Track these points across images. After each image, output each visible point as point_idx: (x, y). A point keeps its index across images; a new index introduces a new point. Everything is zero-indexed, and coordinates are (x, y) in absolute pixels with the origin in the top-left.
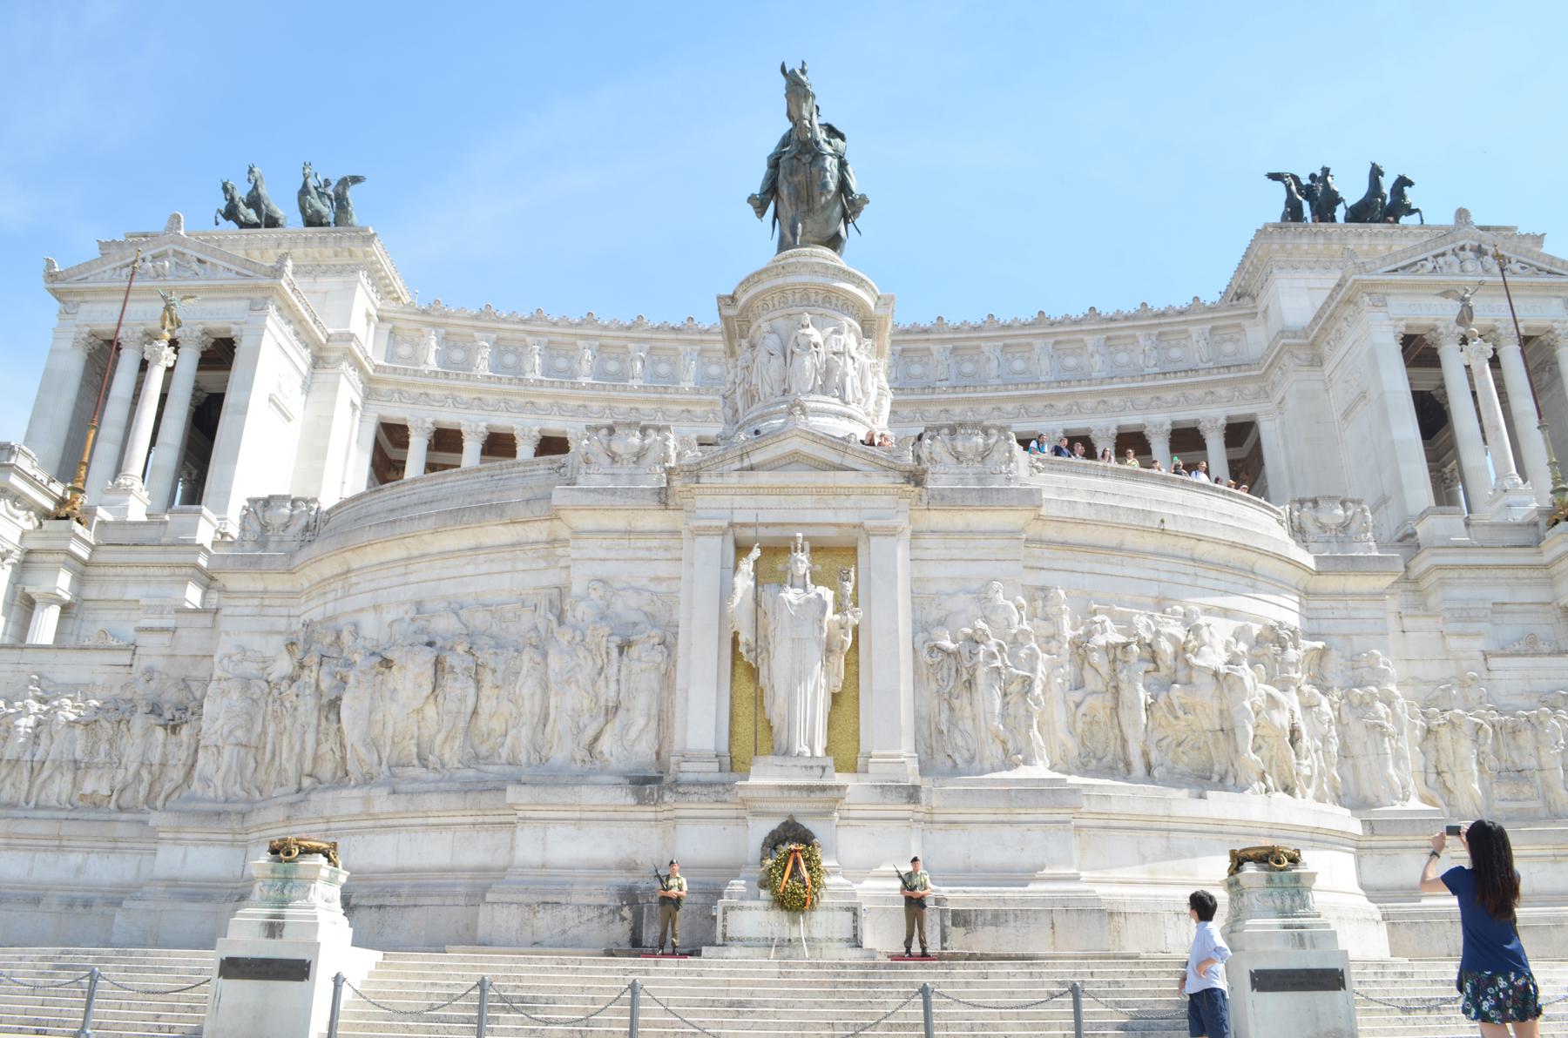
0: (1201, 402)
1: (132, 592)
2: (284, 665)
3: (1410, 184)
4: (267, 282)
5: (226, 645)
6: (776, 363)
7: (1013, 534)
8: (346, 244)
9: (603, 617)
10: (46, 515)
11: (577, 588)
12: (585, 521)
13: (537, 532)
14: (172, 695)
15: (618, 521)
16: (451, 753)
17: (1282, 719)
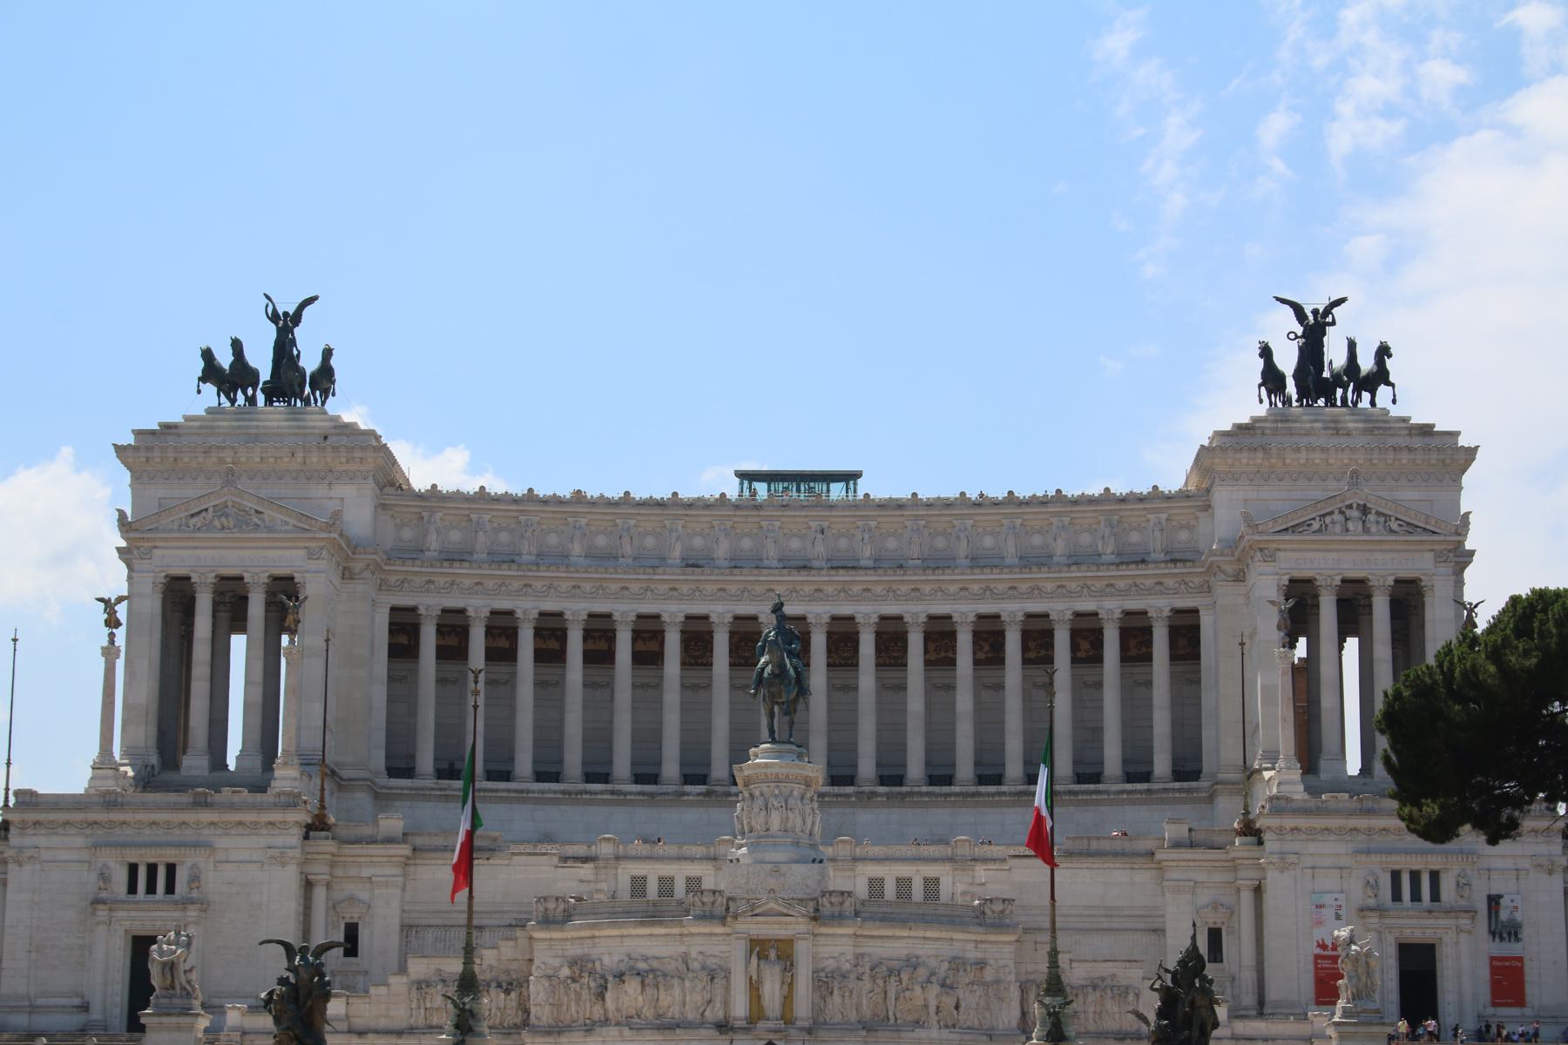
0: (1150, 592)
1: (366, 873)
2: (565, 972)
3: (1390, 356)
4: (324, 535)
5: (537, 962)
6: (763, 813)
7: (849, 936)
8: (357, 454)
9: (704, 968)
10: (309, 828)
11: (694, 955)
12: (694, 930)
13: (676, 931)
14: (503, 977)
15: (707, 930)
16: (648, 1013)
17: (951, 1001)
